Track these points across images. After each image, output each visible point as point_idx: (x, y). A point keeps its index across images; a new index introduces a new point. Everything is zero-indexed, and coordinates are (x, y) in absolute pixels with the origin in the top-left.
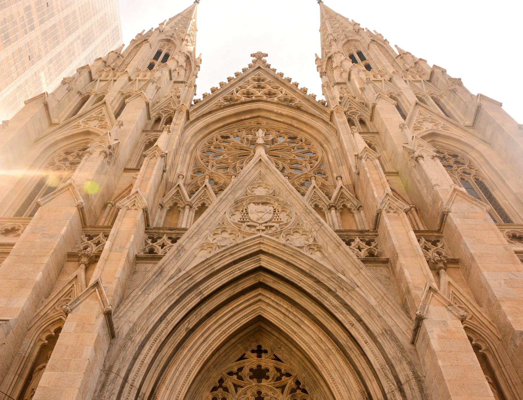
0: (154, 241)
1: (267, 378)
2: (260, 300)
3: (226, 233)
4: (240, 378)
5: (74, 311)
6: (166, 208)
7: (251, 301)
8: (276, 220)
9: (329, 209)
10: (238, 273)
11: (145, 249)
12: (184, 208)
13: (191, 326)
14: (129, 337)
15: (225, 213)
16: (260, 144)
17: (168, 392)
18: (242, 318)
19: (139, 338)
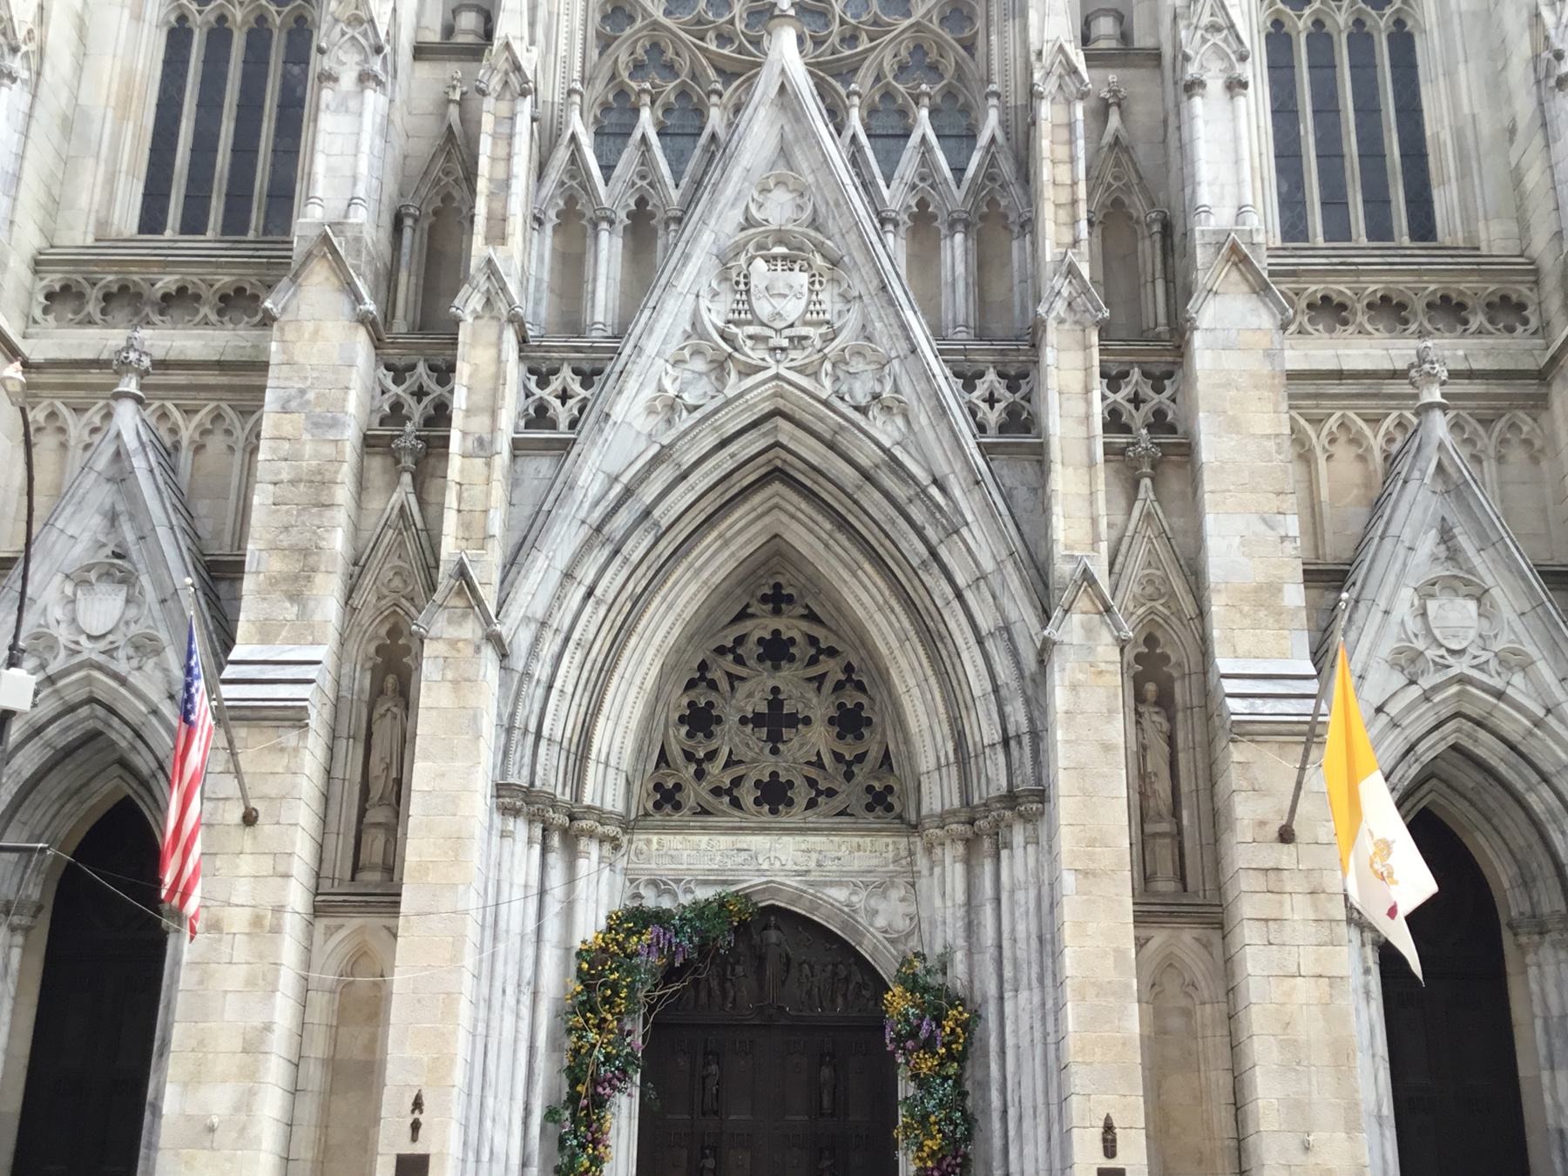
0: (543, 383)
1: (792, 659)
2: (777, 506)
3: (701, 357)
4: (739, 660)
5: (432, 634)
6: (551, 220)
7: (759, 510)
8: (815, 315)
9: (952, 226)
10: (729, 465)
11: (527, 409)
12: (596, 226)
13: (639, 590)
14: (533, 652)
15: (698, 296)
16: (783, 16)
17: (611, 724)
18: (741, 547)
19: (549, 648)
